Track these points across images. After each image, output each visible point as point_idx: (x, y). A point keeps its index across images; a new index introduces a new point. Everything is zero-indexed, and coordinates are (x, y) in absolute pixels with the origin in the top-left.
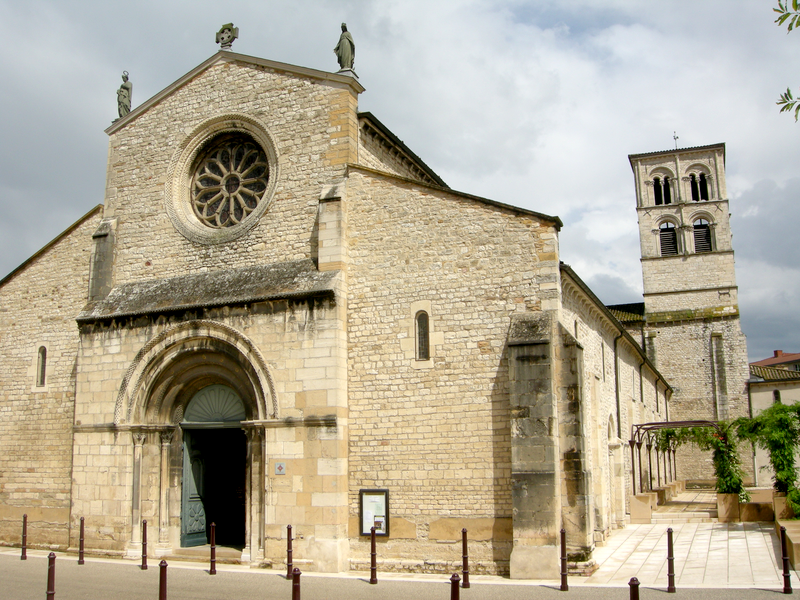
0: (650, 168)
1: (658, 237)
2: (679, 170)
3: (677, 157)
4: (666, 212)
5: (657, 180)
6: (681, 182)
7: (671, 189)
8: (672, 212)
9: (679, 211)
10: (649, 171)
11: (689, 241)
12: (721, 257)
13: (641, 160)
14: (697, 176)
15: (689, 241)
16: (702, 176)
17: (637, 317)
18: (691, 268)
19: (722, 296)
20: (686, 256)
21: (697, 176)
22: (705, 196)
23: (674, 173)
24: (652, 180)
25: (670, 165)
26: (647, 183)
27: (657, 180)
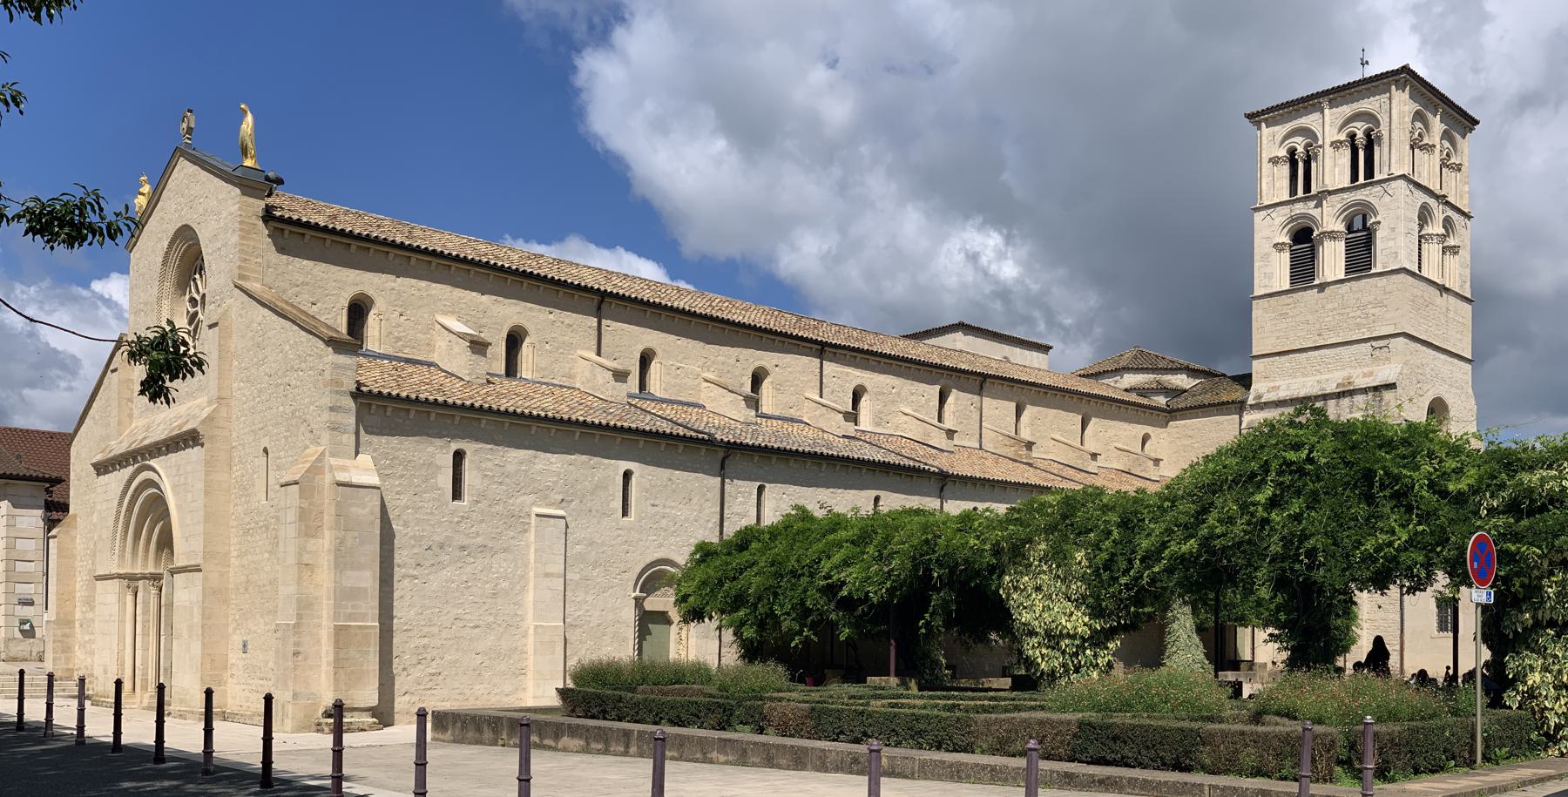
0: (1281, 130)
1: (1286, 256)
2: (1327, 128)
3: (1325, 104)
4: (1299, 208)
5: (1292, 152)
6: (1328, 150)
7: (1313, 165)
8: (1309, 208)
9: (1319, 205)
10: (1279, 138)
11: (1332, 259)
12: (1382, 281)
13: (1266, 120)
14: (1360, 134)
15: (1332, 259)
16: (1368, 134)
17: (1237, 394)
18: (1330, 306)
19: (1377, 352)
20: (1322, 287)
21: (1360, 134)
22: (1370, 173)
23: (1319, 136)
24: (1283, 153)
25: (1310, 121)
26: (1274, 161)
27: (1292, 152)
